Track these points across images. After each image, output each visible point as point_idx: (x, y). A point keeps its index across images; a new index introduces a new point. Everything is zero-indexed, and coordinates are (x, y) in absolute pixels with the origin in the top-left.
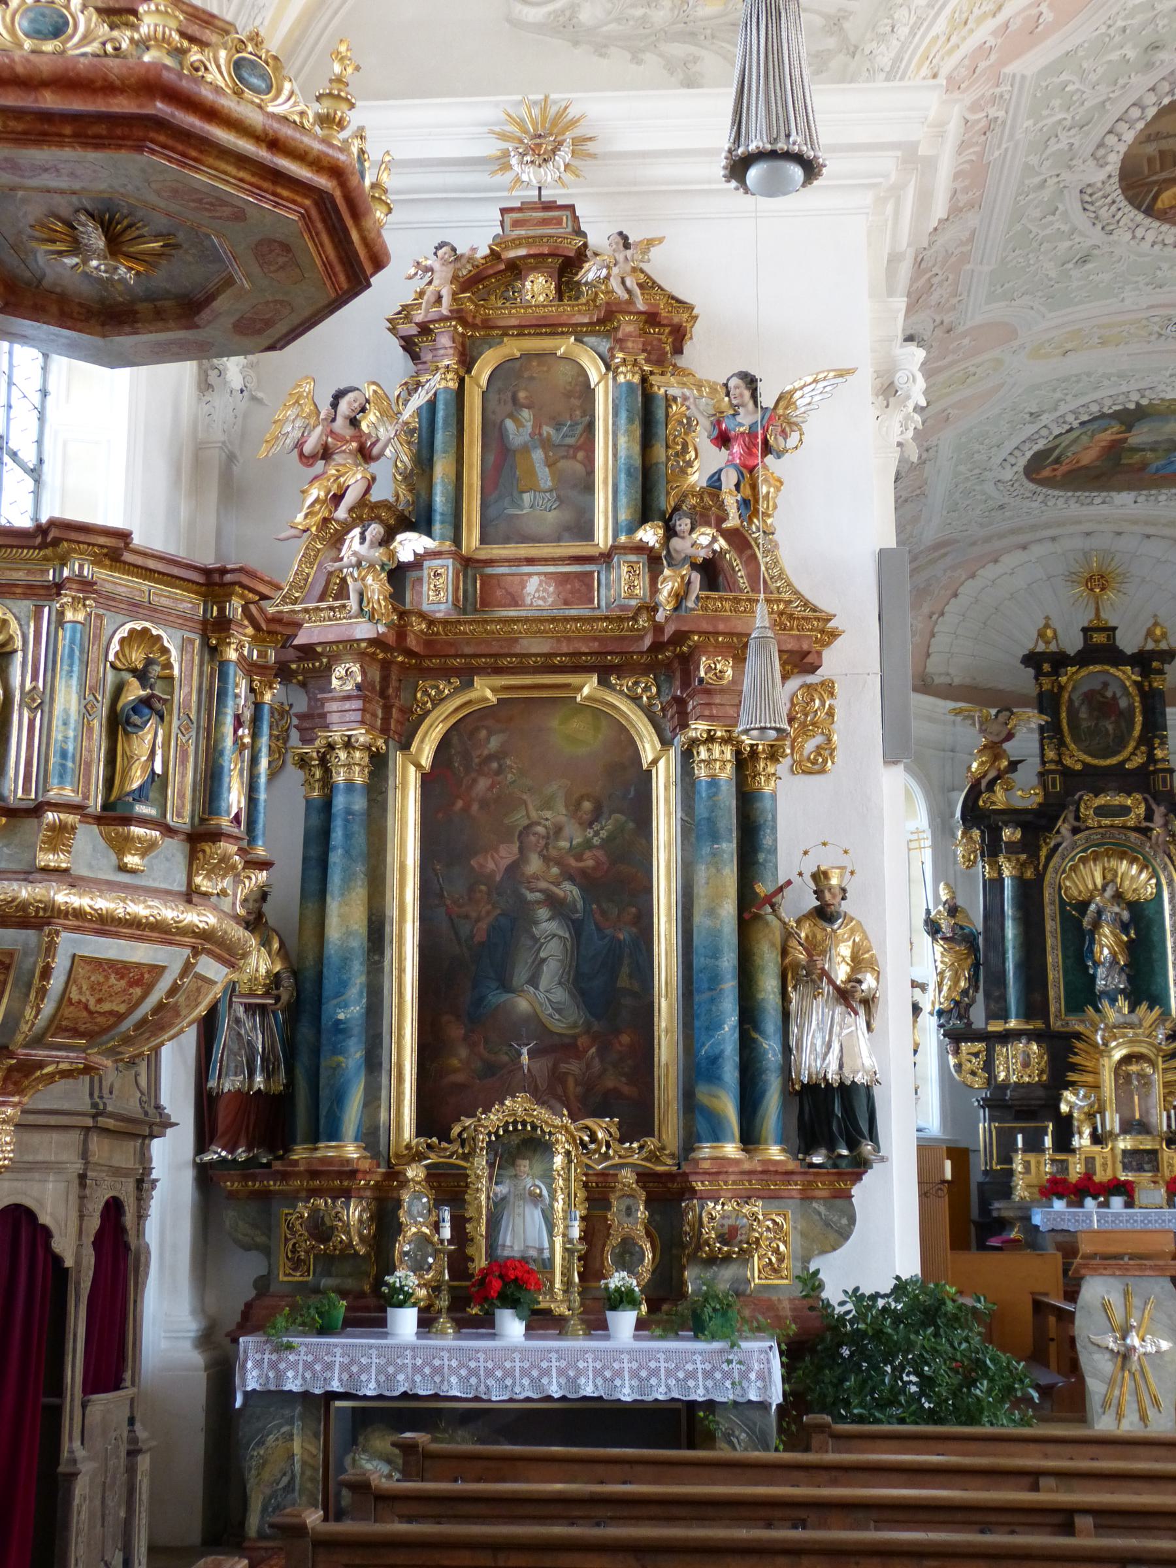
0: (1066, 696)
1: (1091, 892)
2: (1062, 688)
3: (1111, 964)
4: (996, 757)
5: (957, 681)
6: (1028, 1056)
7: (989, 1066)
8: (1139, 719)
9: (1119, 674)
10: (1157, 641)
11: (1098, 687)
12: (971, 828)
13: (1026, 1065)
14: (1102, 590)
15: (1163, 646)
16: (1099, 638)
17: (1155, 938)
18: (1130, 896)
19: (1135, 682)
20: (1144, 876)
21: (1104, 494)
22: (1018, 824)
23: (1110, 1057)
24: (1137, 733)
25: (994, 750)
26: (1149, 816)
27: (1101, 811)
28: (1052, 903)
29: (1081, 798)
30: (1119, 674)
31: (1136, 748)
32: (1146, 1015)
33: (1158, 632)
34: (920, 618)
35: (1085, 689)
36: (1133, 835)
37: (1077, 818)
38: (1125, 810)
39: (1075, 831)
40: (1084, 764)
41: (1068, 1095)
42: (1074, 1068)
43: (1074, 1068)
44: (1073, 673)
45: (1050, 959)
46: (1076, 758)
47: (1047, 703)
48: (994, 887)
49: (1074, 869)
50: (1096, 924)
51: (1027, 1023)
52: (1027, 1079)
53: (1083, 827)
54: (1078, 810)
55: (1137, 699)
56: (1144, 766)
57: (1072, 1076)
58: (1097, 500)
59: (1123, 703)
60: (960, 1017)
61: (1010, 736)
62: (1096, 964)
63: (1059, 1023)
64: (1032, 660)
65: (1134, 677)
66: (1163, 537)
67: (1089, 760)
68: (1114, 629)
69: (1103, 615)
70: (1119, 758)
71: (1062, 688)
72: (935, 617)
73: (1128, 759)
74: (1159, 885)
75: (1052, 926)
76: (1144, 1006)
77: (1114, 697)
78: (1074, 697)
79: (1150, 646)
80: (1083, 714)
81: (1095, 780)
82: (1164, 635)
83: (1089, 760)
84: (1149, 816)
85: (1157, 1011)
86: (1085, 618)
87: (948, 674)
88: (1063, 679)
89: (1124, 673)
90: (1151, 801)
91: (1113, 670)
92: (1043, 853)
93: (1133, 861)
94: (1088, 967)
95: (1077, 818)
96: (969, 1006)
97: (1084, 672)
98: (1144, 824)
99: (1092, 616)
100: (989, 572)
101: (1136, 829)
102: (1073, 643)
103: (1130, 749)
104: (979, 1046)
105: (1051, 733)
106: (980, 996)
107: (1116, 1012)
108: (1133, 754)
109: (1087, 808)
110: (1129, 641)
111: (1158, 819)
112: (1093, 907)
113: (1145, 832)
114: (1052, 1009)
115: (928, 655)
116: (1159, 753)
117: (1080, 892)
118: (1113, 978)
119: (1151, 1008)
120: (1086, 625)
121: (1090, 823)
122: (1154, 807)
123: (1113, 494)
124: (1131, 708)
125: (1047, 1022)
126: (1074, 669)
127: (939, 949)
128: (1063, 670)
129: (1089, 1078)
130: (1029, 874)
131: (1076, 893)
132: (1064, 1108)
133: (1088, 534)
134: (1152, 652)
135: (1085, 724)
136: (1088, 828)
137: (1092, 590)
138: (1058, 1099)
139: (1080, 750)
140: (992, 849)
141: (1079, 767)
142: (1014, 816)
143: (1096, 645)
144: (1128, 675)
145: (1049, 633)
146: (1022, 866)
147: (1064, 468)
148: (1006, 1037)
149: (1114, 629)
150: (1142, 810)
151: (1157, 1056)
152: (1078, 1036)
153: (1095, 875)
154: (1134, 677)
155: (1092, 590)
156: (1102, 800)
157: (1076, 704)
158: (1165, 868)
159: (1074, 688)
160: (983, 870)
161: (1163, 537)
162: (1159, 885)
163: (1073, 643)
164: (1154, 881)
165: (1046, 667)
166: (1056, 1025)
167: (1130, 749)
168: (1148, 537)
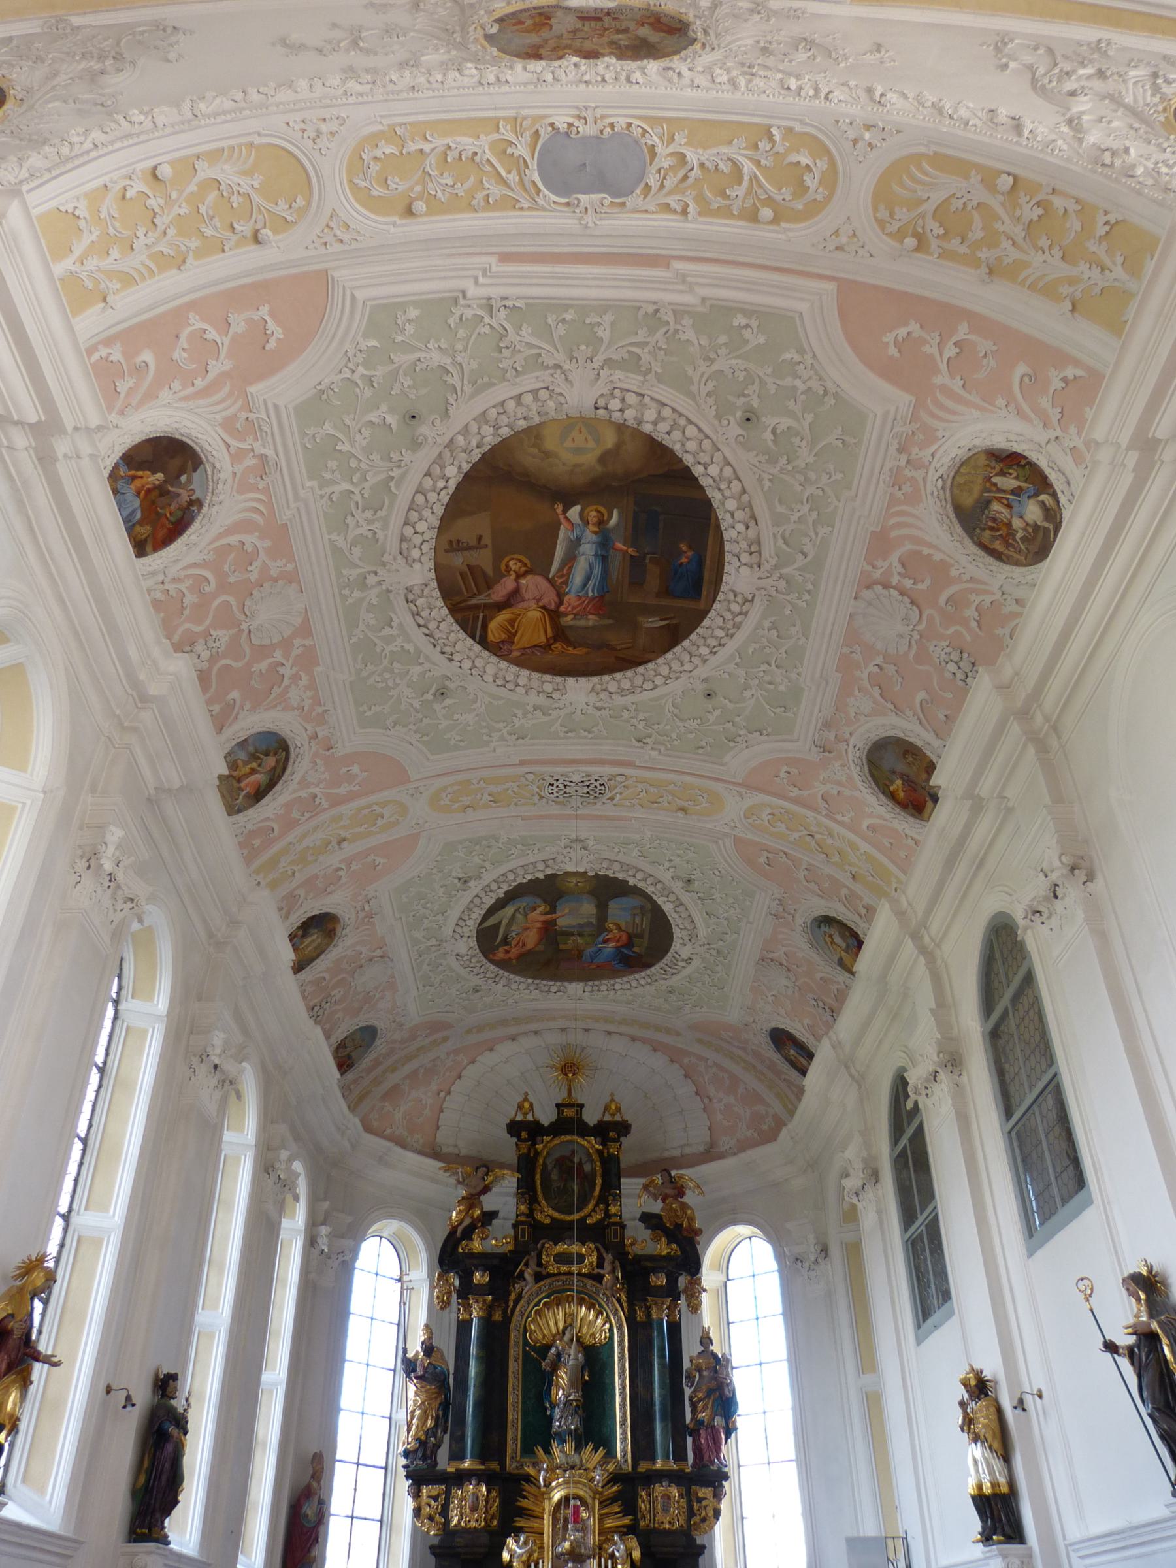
0: (541, 1161)
1: (554, 1336)
2: (537, 1154)
3: (565, 1404)
4: (471, 1207)
5: (464, 1152)
6: (477, 1498)
7: (445, 1511)
8: (599, 1181)
9: (584, 1143)
10: (613, 1115)
11: (568, 1154)
12: (448, 1272)
13: (474, 1509)
14: (574, 1075)
15: (617, 1118)
16: (568, 1112)
17: (607, 1381)
18: (588, 1341)
19: (597, 1150)
20: (600, 1321)
21: (558, 983)
22: (485, 1268)
23: (550, 1499)
24: (597, 1193)
25: (471, 1200)
26: (600, 1265)
27: (562, 1258)
28: (517, 1345)
29: (543, 1244)
30: (584, 1143)
31: (596, 1205)
32: (592, 1457)
33: (613, 1107)
34: (429, 1094)
35: (557, 1155)
36: (589, 1282)
37: (540, 1264)
38: (581, 1258)
39: (538, 1277)
40: (553, 1219)
41: (510, 1541)
42: (522, 1512)
43: (522, 1512)
44: (548, 1142)
45: (510, 1399)
46: (546, 1213)
47: (526, 1167)
48: (463, 1328)
49: (538, 1312)
50: (555, 1367)
51: (483, 1464)
52: (473, 1524)
53: (544, 1273)
54: (539, 1256)
55: (598, 1164)
56: (601, 1221)
57: (520, 1522)
58: (554, 989)
59: (587, 1168)
60: (424, 1458)
61: (486, 1190)
62: (553, 1406)
63: (514, 1465)
64: (514, 1128)
65: (597, 1146)
66: (621, 1034)
67: (556, 1215)
68: (581, 1106)
69: (573, 1095)
70: (582, 1214)
71: (537, 1154)
72: (442, 1094)
73: (590, 1215)
74: (611, 1330)
75: (515, 1367)
76: (590, 1447)
77: (580, 1163)
78: (548, 1162)
79: (607, 1118)
80: (554, 1177)
81: (558, 1232)
82: (618, 1110)
83: (556, 1215)
84: (600, 1265)
85: (601, 1452)
86: (560, 1096)
87: (456, 1146)
88: (539, 1147)
89: (589, 1142)
90: (602, 1250)
91: (579, 1140)
92: (513, 1297)
93: (590, 1307)
94: (546, 1409)
95: (540, 1264)
96: (437, 1446)
97: (557, 1141)
98: (596, 1271)
99: (566, 1095)
100: (488, 1059)
101: (590, 1276)
102: (546, 1116)
103: (591, 1206)
104: (435, 1489)
105: (526, 1189)
106: (447, 1438)
107: (563, 1452)
108: (593, 1210)
109: (548, 1256)
110: (591, 1117)
111: (607, 1267)
112: (553, 1350)
113: (599, 1278)
114: (509, 1451)
115: (438, 1128)
116: (613, 1210)
117: (544, 1336)
118: (566, 1419)
119: (596, 1450)
120: (560, 1102)
121: (552, 1269)
122: (605, 1255)
123: (566, 984)
124: (593, 1172)
125: (503, 1465)
126: (549, 1138)
127: (412, 1389)
128: (539, 1138)
129: (535, 1524)
130: (497, 1316)
131: (540, 1337)
132: (506, 1556)
133: (563, 1030)
134: (609, 1123)
135: (555, 1185)
136: (549, 1275)
137: (566, 1075)
138: (502, 1545)
139: (549, 1206)
140: (466, 1291)
141: (548, 1221)
142: (486, 1260)
143: (567, 1118)
144: (592, 1144)
145: (526, 1105)
146: (489, 1309)
147: (515, 952)
148: (460, 1478)
149: (581, 1106)
150: (594, 1258)
151: (594, 1499)
152: (528, 1479)
153: (555, 1319)
154: (597, 1146)
155: (566, 1075)
156: (562, 1248)
157: (550, 1168)
158: (616, 1314)
159: (548, 1154)
160: (455, 1313)
161: (621, 1034)
162: (611, 1330)
163: (546, 1116)
164: (607, 1326)
165: (524, 1134)
166: (511, 1466)
167: (591, 1206)
168: (609, 1033)
